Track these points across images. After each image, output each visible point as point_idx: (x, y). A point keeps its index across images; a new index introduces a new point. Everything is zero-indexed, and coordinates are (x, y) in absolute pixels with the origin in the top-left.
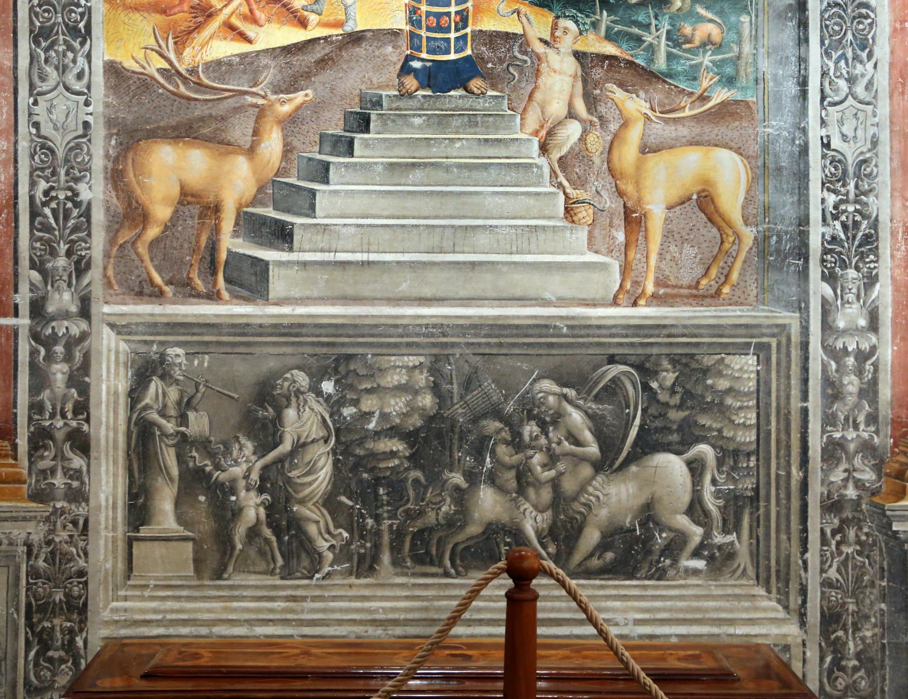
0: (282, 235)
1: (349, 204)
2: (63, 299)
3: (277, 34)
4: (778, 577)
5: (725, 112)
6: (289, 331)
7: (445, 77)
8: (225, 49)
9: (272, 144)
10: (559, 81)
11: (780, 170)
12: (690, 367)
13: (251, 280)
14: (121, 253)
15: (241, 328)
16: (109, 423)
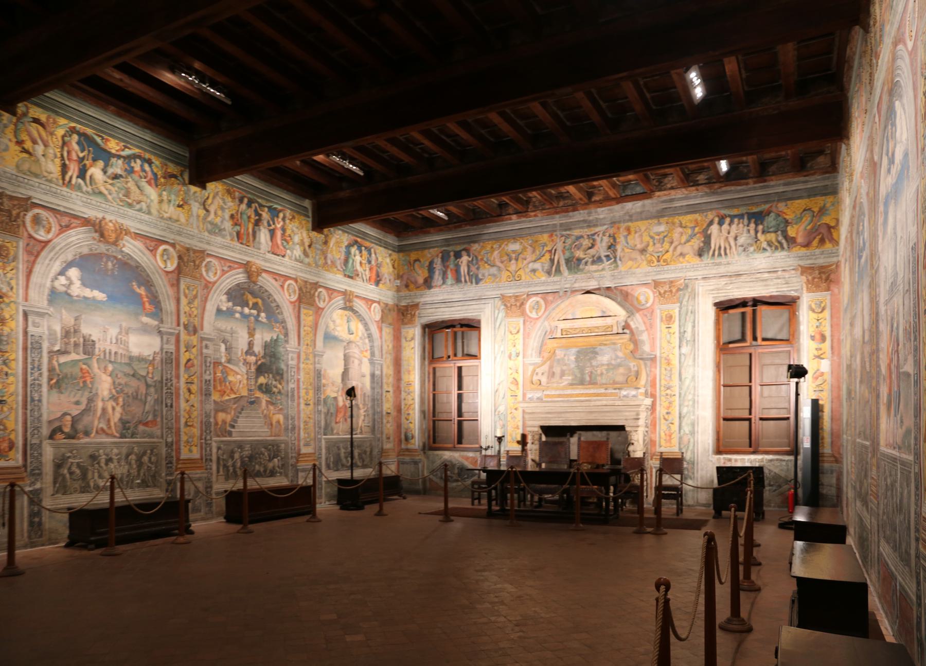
0: (233, 427)
1: (242, 423)
2: (208, 437)
3: (233, 396)
4: (286, 476)
5: (281, 409)
6: (235, 441)
7: (252, 403)
8: (227, 398)
9: (233, 413)
10: (264, 404)
11: (286, 418)
12: (278, 446)
13: (230, 434)
14: (215, 429)
15: (230, 441)
16: (214, 458)
